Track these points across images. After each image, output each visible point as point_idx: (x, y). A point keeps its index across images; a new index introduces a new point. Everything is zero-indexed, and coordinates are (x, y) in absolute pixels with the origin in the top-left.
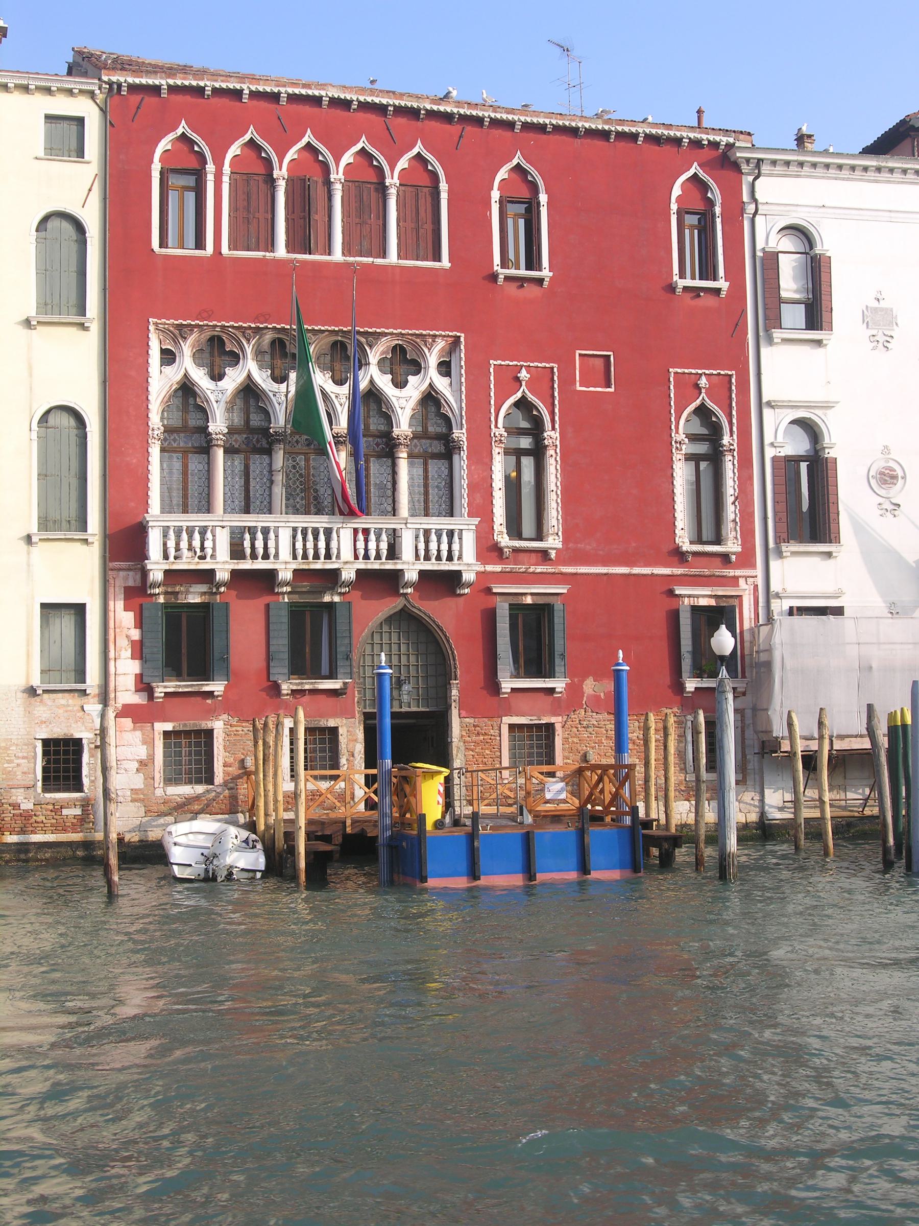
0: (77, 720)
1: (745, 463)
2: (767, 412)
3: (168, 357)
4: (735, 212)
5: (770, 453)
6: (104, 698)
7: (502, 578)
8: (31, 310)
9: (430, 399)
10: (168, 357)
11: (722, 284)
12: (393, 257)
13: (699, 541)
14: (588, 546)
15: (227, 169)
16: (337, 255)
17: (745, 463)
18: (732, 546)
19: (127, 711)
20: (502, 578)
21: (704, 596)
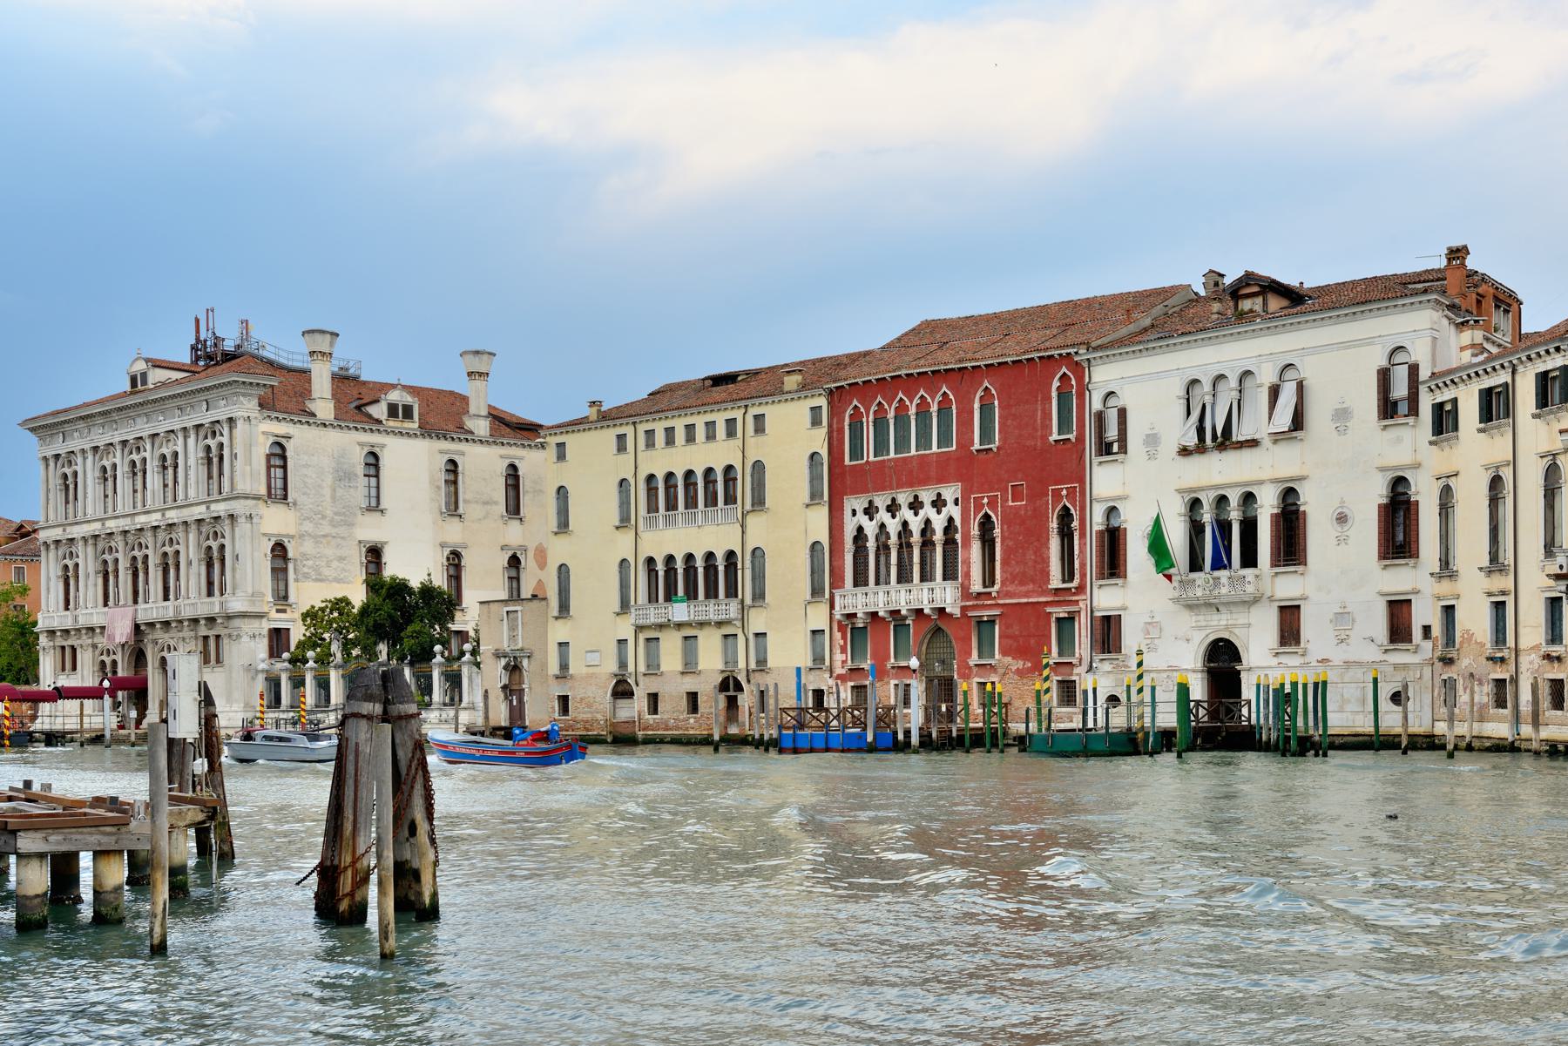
0: (824, 682)
1: (1083, 535)
2: (1095, 505)
3: (854, 513)
4: (1083, 389)
5: (1096, 528)
6: (831, 672)
7: (974, 607)
8: (807, 501)
9: (951, 520)
10: (854, 513)
11: (1072, 437)
12: (935, 449)
13: (1064, 581)
14: (1011, 588)
15: (871, 418)
16: (913, 452)
17: (1083, 535)
18: (1076, 583)
19: (839, 677)
20: (974, 607)
21: (1061, 612)
